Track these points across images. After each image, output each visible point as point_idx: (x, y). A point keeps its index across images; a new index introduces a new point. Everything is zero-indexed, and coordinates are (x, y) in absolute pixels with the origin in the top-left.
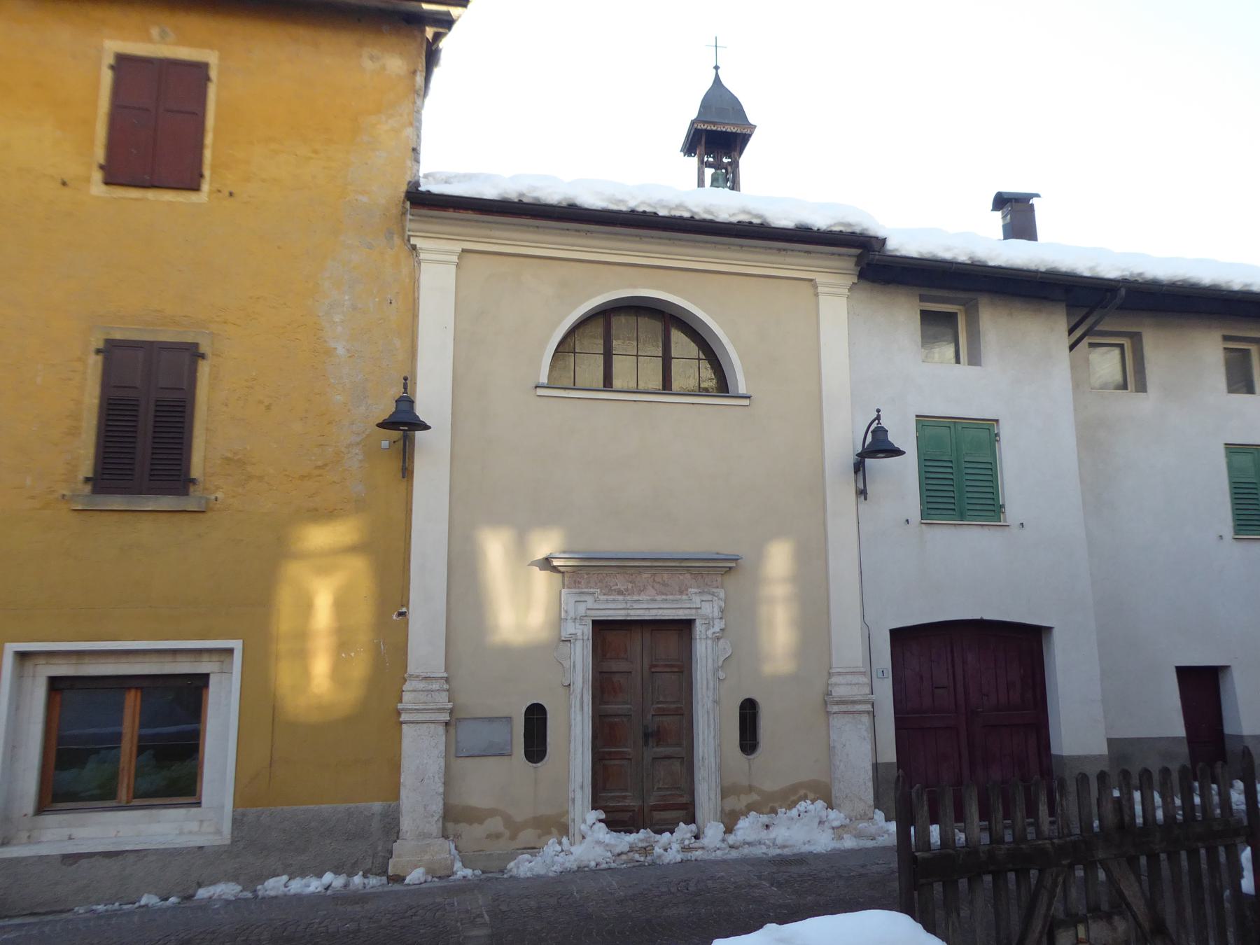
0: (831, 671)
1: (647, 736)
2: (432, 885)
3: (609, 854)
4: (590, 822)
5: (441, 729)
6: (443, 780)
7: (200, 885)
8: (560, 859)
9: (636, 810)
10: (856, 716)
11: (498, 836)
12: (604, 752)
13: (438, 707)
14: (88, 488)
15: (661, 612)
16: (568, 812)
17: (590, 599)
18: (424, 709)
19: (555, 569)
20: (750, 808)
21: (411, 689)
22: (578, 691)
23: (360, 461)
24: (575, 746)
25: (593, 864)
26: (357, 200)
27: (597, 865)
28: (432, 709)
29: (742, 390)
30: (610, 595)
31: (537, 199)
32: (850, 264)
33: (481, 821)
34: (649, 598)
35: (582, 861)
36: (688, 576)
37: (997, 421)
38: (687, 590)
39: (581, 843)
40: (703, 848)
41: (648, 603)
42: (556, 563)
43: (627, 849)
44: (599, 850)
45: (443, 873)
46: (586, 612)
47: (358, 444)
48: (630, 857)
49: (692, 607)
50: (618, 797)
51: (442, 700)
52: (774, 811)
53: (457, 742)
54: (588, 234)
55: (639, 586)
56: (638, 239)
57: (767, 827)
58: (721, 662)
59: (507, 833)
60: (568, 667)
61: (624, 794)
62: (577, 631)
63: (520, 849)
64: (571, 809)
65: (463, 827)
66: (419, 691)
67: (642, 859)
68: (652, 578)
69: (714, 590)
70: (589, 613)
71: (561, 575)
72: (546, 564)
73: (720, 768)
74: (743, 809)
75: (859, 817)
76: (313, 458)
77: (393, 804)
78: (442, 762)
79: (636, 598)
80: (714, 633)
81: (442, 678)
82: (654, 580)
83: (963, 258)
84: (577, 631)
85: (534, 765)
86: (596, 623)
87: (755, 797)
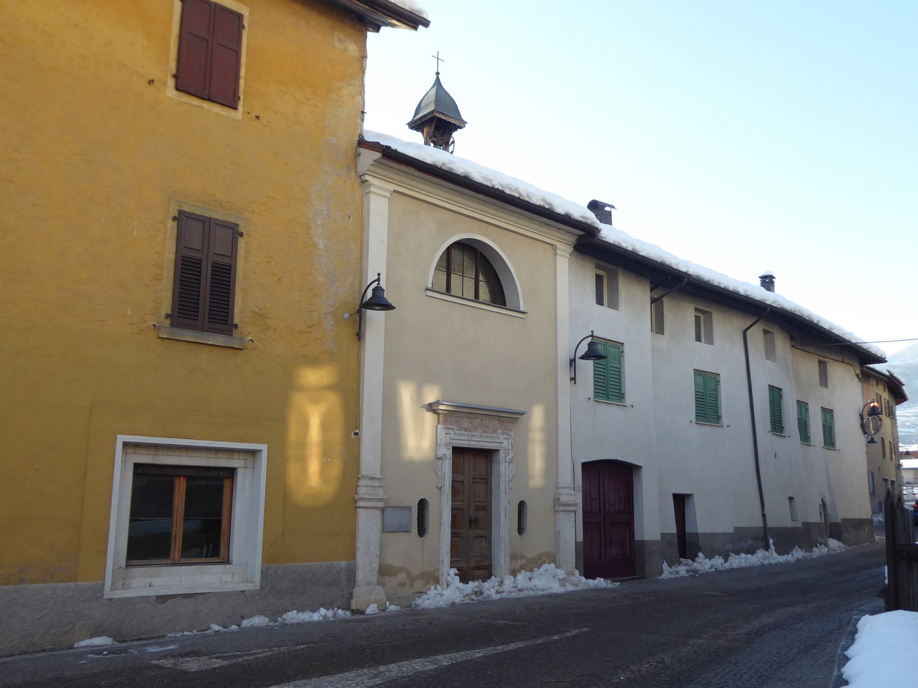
0: (557, 486)
1: (471, 522)
5: (378, 513)
7: (243, 618)
10: (570, 513)
11: (402, 585)
14: (168, 322)
18: (373, 499)
20: (522, 568)
26: (330, 140)
29: (522, 309)
31: (451, 169)
36: (497, 422)
37: (623, 344)
39: (447, 588)
47: (331, 313)
52: (532, 570)
56: (484, 203)
59: (408, 583)
72: (431, 407)
74: (518, 567)
79: (473, 434)
83: (630, 248)
87: (524, 561)
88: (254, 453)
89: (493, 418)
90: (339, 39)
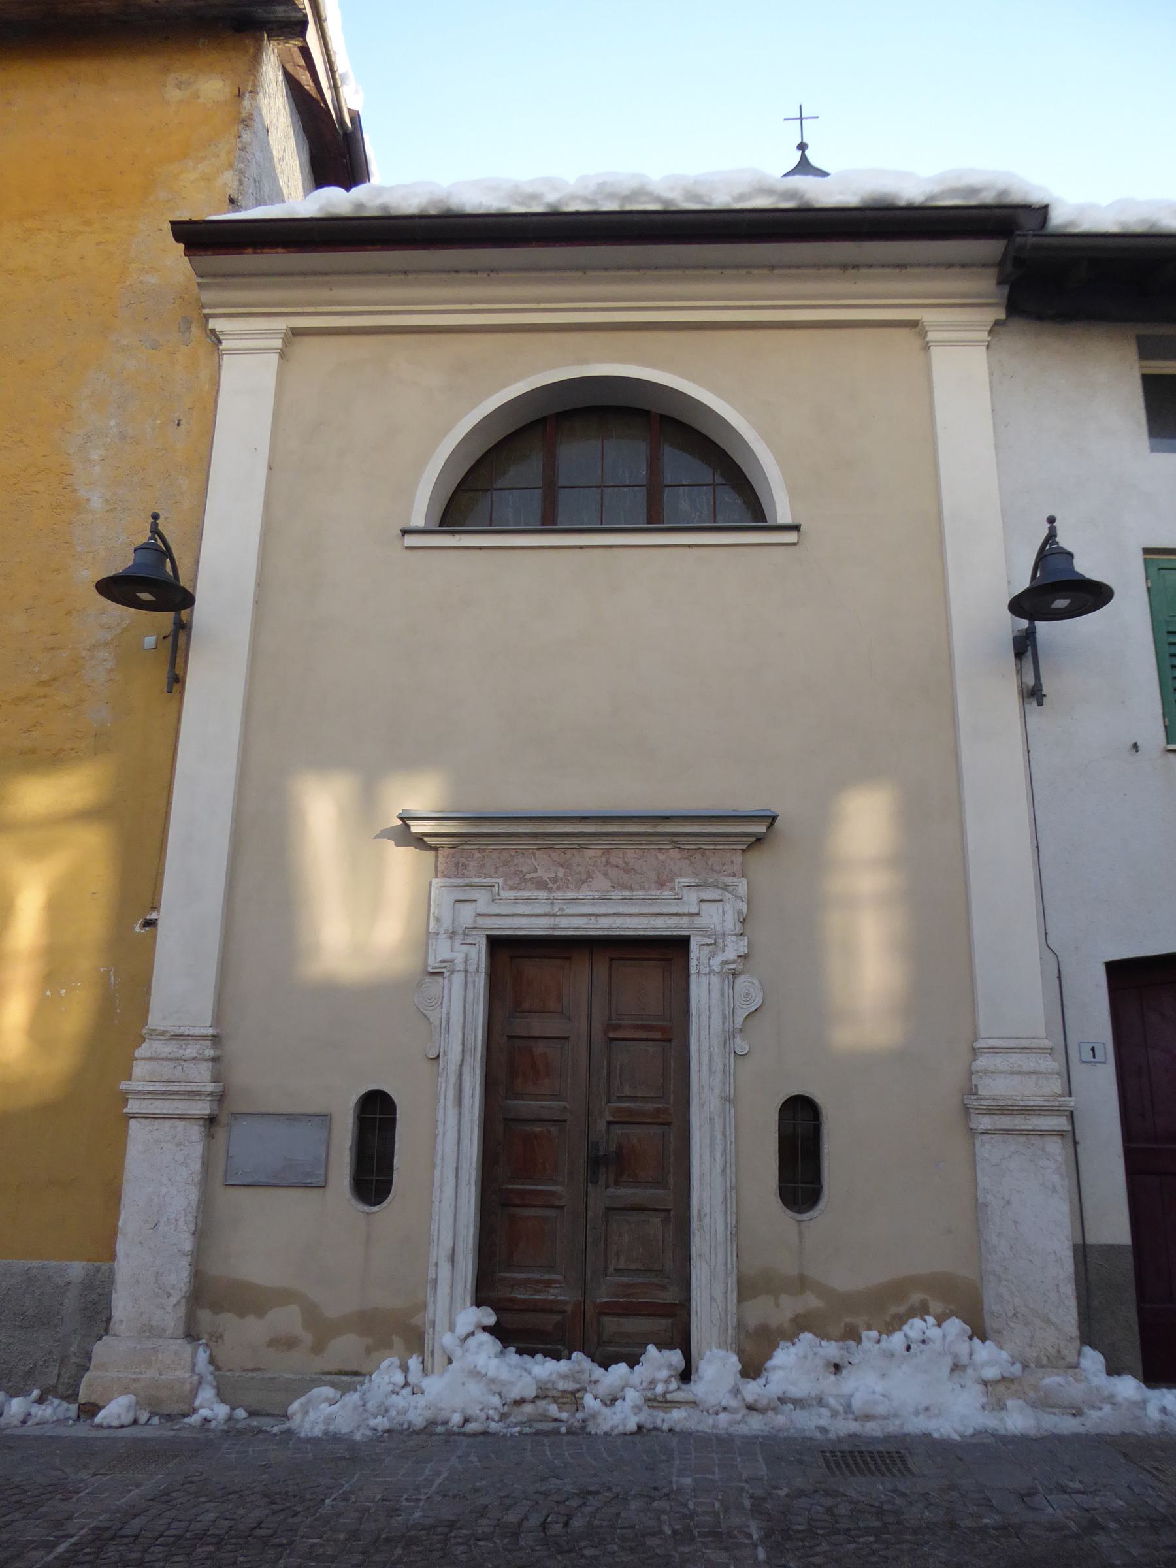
0: (976, 1045)
2: (148, 1432)
3: (496, 1401)
4: (462, 1328)
5: (195, 1131)
6: (192, 1227)
8: (399, 1401)
9: (569, 1308)
11: (288, 1343)
12: (512, 1191)
13: (189, 1089)
15: (619, 921)
16: (424, 1306)
17: (482, 897)
18: (164, 1093)
19: (419, 841)
20: (802, 1324)
21: (149, 1055)
22: (453, 1067)
23: (111, 670)
24: (442, 1177)
25: (457, 1418)
26: (142, 282)
27: (466, 1421)
28: (177, 1093)
29: (783, 515)
30: (523, 889)
31: (385, 207)
32: (985, 284)
33: (261, 1312)
34: (597, 895)
35: (441, 1409)
36: (675, 853)
38: (672, 880)
39: (444, 1371)
40: (694, 1404)
41: (593, 904)
42: (417, 828)
43: (531, 1392)
44: (475, 1389)
45: (175, 1409)
46: (475, 922)
47: (106, 644)
48: (540, 1411)
49: (680, 912)
50: (538, 1281)
51: (201, 1077)
52: (852, 1334)
53: (228, 1157)
54: (492, 275)
55: (579, 873)
57: (837, 1368)
58: (739, 1021)
59: (308, 1338)
60: (437, 1023)
61: (547, 1277)
62: (455, 955)
63: (329, 1373)
64: (430, 1300)
65: (227, 1320)
66: (163, 1059)
67: (564, 1416)
68: (603, 860)
69: (729, 880)
70: (481, 922)
71: (433, 853)
72: (405, 835)
73: (736, 1233)
75: (1045, 1361)
76: (37, 669)
77: (105, 1267)
78: (194, 1194)
79: (571, 894)
80: (724, 963)
81: (204, 1037)
82: (608, 863)
84: (455, 955)
85: (367, 1208)
86: (497, 944)
87: (812, 1301)
89: (651, 842)
90: (179, 85)
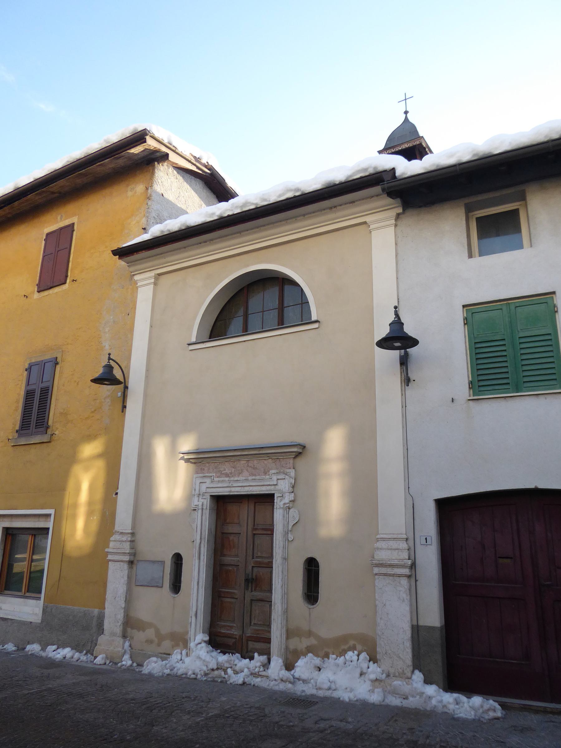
1: (247, 581)
5: (126, 566)
7: (29, 643)
9: (237, 637)
10: (397, 579)
14: (16, 435)
17: (208, 480)
18: (116, 553)
20: (309, 650)
29: (314, 318)
34: (244, 478)
36: (270, 460)
37: (554, 293)
38: (269, 471)
40: (267, 677)
44: (198, 663)
49: (271, 484)
52: (327, 656)
53: (136, 575)
56: (239, 234)
57: (320, 669)
58: (290, 527)
59: (156, 640)
61: (231, 625)
63: (161, 653)
66: (117, 541)
68: (247, 464)
69: (288, 470)
73: (286, 612)
74: (304, 650)
75: (397, 674)
79: (236, 479)
80: (285, 504)
82: (248, 466)
83: (466, 157)
87: (313, 641)
88: (48, 516)
89: (261, 457)
